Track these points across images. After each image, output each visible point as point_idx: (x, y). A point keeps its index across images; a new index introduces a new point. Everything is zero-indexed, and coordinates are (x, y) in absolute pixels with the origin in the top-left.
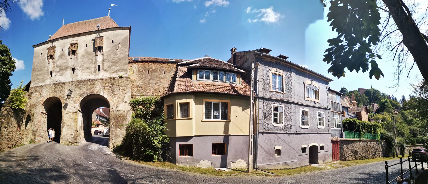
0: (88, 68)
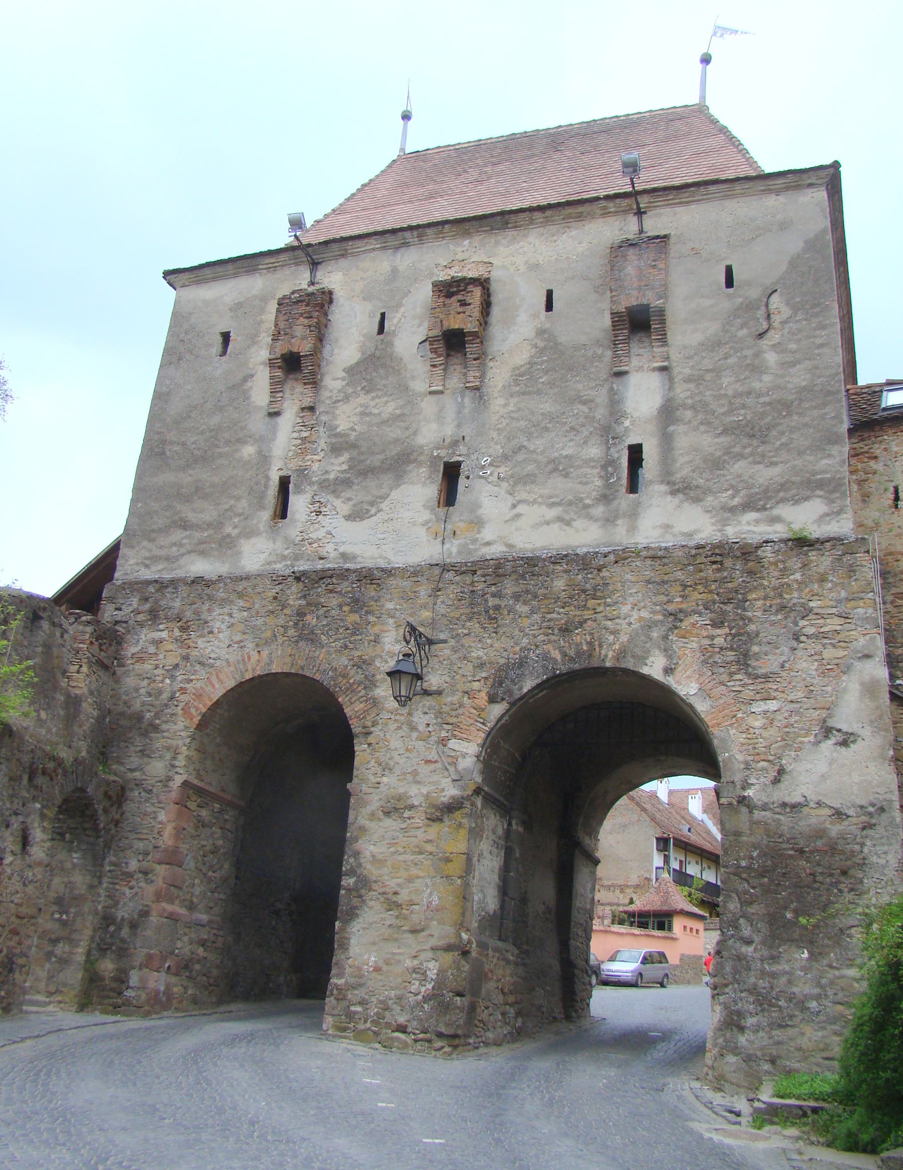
0: (559, 467)
